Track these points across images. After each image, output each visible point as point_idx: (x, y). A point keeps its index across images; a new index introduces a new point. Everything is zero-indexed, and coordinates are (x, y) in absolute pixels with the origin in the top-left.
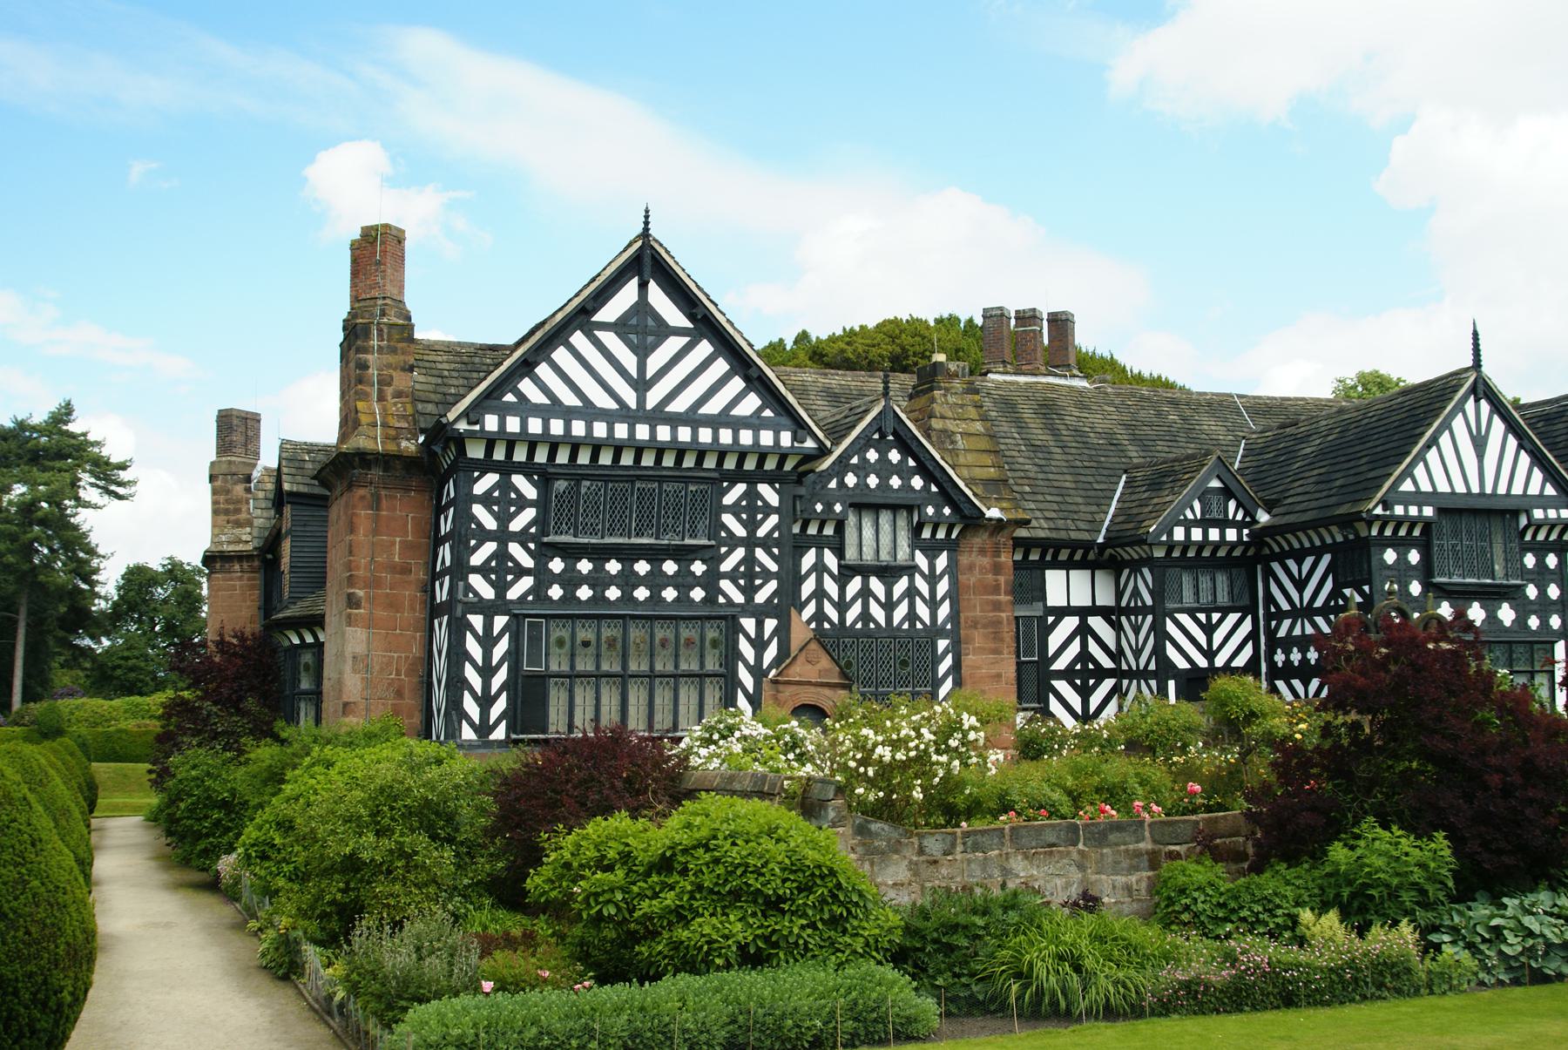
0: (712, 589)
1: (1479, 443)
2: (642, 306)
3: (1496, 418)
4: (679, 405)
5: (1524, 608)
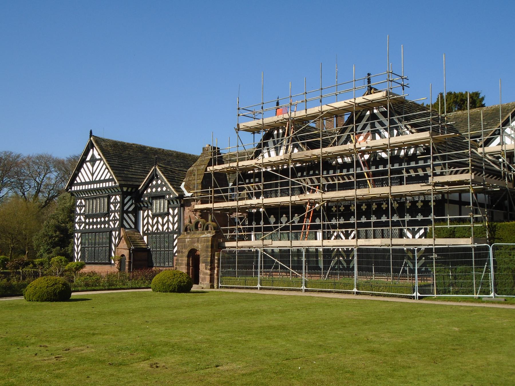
0: (109, 225)
2: (93, 156)
4: (98, 179)
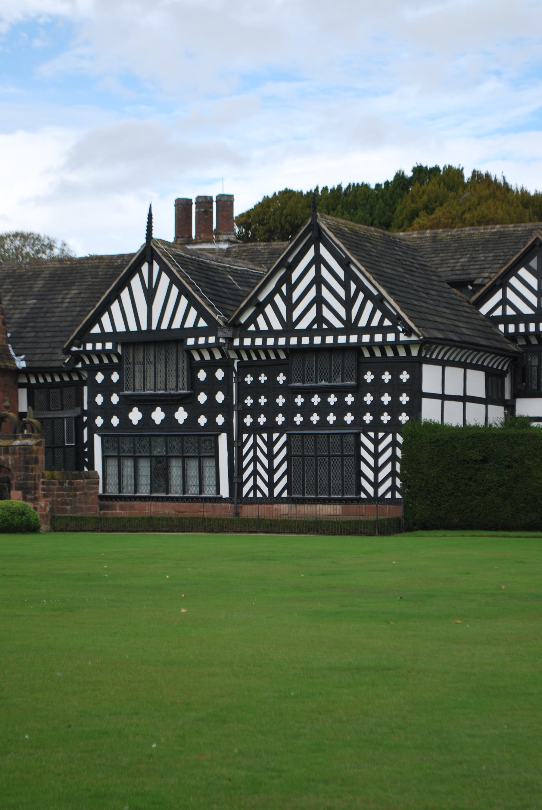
1: (150, 294)
3: (164, 276)
5: (194, 410)
